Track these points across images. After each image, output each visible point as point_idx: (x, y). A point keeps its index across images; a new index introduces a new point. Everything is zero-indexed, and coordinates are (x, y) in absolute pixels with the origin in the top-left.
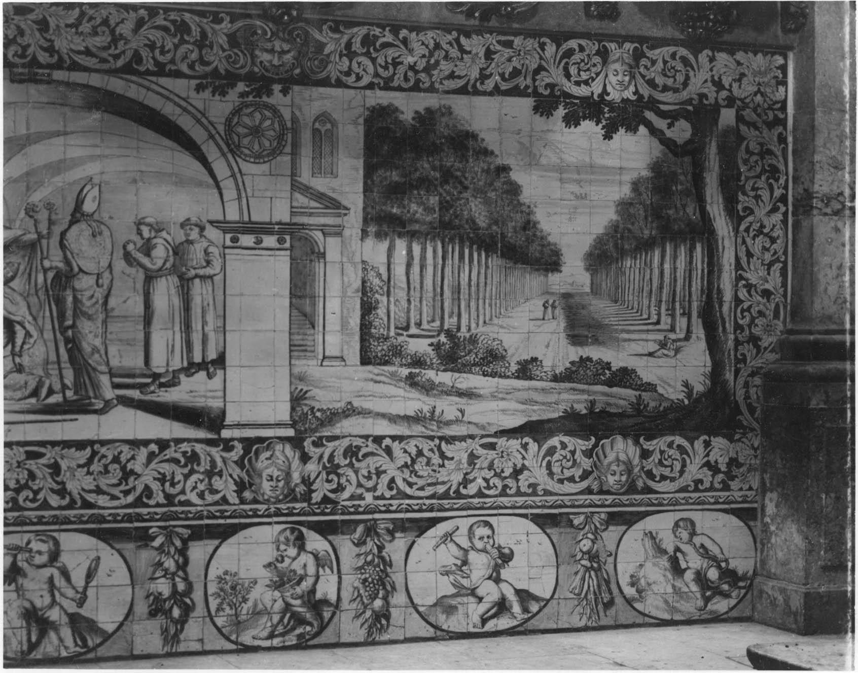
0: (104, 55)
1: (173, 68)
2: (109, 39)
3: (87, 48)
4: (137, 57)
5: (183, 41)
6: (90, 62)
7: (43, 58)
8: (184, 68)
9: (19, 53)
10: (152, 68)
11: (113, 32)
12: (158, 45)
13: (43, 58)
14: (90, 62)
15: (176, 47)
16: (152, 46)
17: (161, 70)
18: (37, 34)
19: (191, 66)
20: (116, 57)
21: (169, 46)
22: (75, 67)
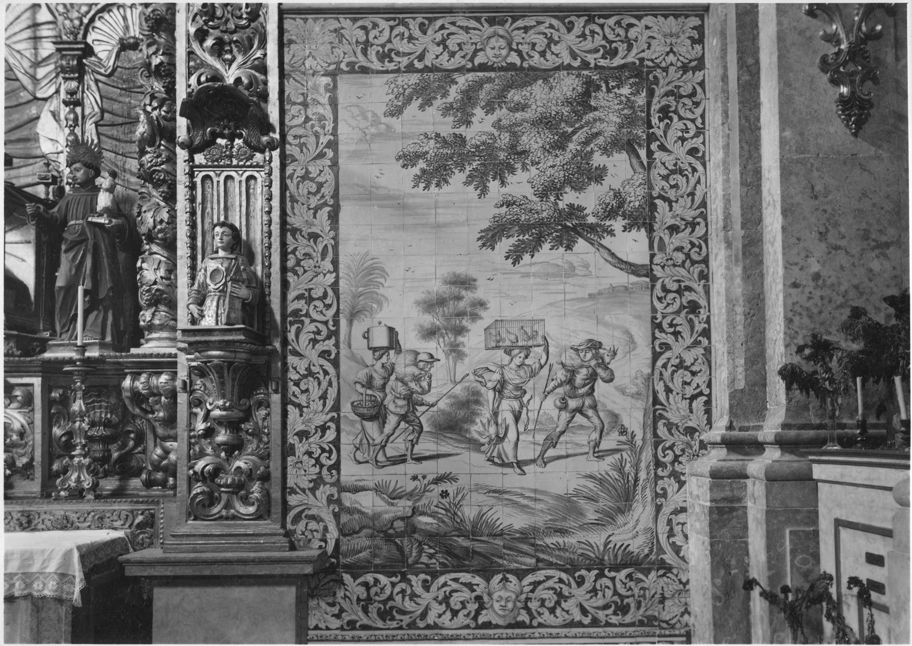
0: (324, 384)
1: (331, 323)
2: (311, 379)
3: (320, 398)
4: (324, 354)
5: (307, 315)
6: (332, 393)
7: (330, 435)
8: (331, 312)
9: (327, 455)
10: (333, 341)
11: (305, 376)
12: (312, 336)
13: (330, 435)
14: (332, 393)
15: (313, 321)
16: (314, 342)
17: (334, 333)
18: (311, 440)
19: (328, 306)
20: (326, 373)
21: (312, 327)
22: (336, 407)
